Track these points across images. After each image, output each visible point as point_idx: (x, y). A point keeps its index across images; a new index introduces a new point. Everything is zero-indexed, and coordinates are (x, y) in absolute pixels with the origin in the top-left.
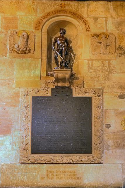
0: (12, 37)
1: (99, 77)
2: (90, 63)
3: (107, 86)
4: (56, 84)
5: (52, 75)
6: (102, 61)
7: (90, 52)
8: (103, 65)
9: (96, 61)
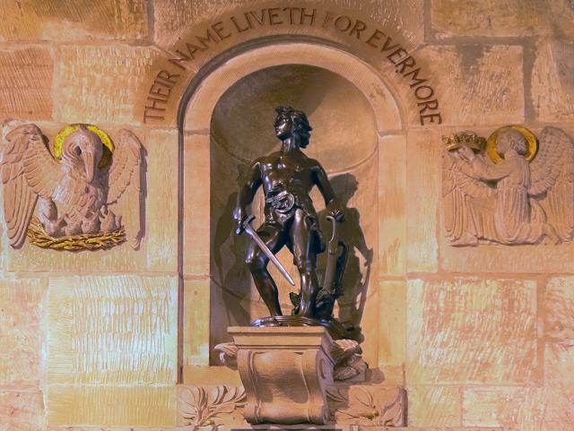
0: (21, 164)
1: (486, 365)
2: (442, 296)
3: (530, 414)
4: (251, 407)
5: (231, 361)
6: (504, 284)
7: (438, 233)
8: (511, 302)
9: (469, 281)
